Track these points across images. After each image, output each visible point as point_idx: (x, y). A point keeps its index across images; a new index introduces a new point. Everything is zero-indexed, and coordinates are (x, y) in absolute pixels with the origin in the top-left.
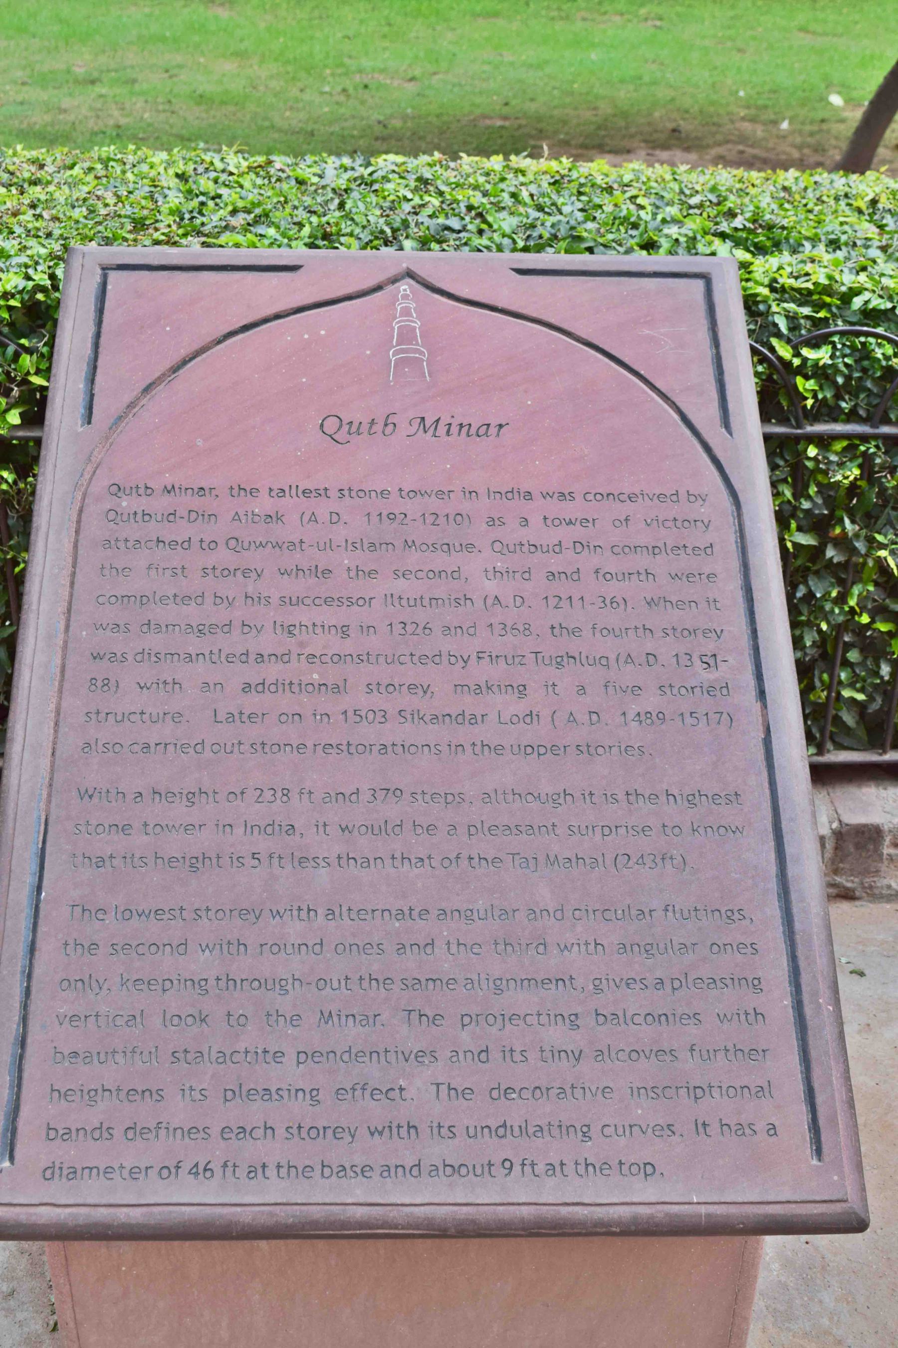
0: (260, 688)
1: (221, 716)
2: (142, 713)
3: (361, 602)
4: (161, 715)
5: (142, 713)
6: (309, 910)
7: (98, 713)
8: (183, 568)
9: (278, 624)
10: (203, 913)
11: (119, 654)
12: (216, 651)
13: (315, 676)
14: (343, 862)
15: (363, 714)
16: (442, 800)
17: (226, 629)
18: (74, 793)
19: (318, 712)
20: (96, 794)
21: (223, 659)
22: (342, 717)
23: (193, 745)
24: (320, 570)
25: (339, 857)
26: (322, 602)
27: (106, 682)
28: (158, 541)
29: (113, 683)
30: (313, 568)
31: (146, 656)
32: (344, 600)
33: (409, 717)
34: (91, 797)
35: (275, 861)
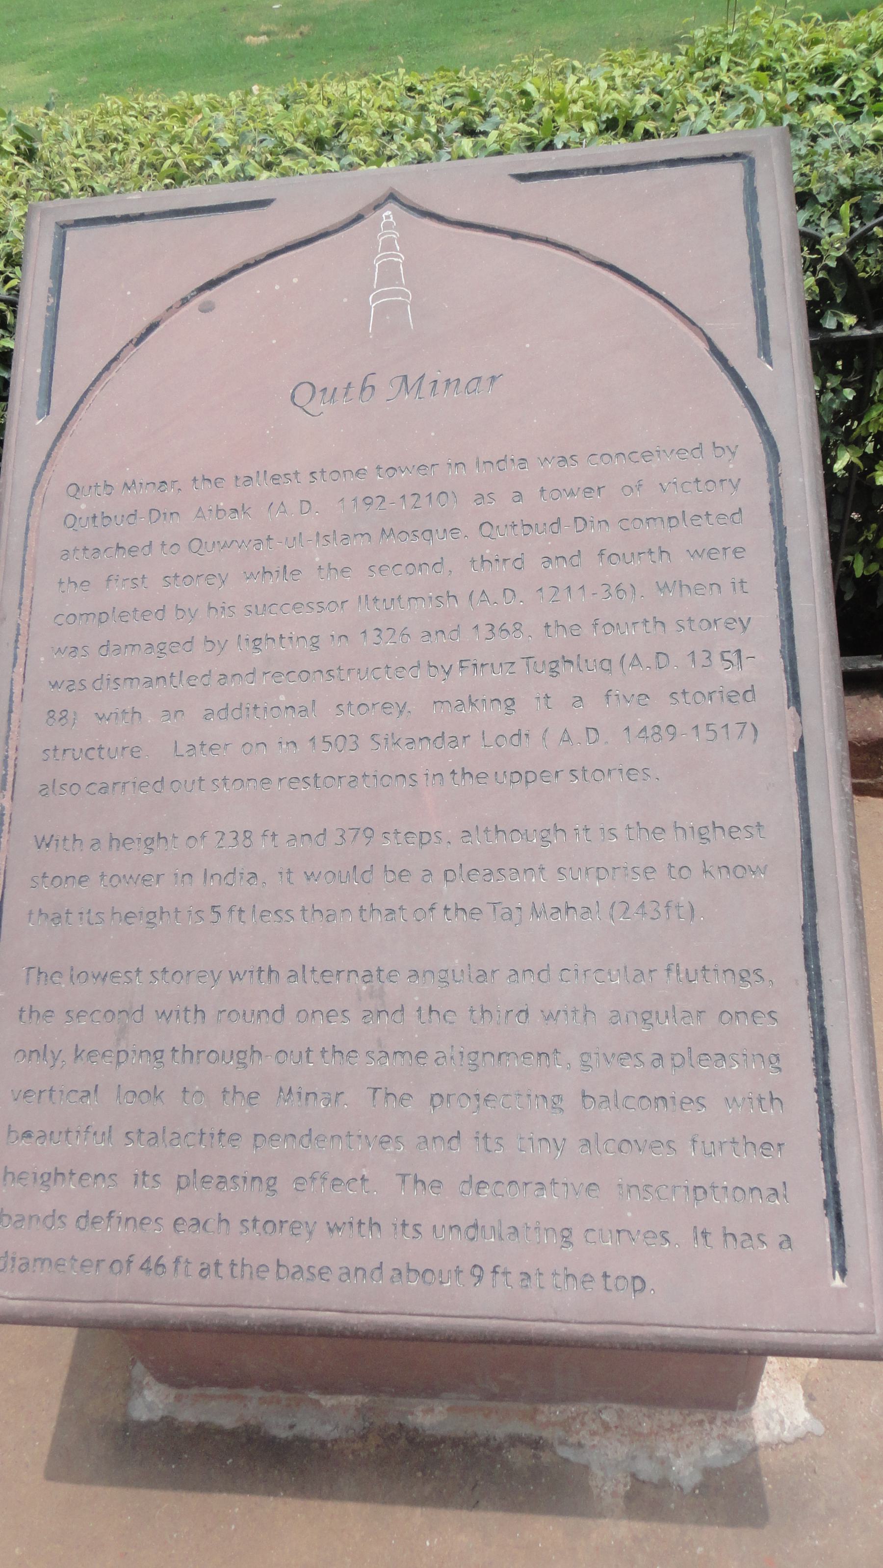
0: (223, 713)
1: (183, 749)
2: (101, 748)
3: (333, 606)
4: (120, 750)
5: (101, 748)
6: (270, 971)
7: (55, 750)
8: (144, 577)
9: (243, 638)
10: (159, 975)
11: (77, 682)
12: (177, 673)
13: (282, 698)
14: (308, 914)
15: (332, 740)
16: (416, 840)
17: (188, 646)
18: (32, 841)
19: (284, 741)
20: (53, 843)
21: (184, 681)
22: (309, 744)
23: (152, 783)
24: (289, 570)
25: (304, 910)
26: (290, 607)
27: (64, 714)
28: (118, 548)
29: (71, 716)
30: (281, 570)
31: (105, 682)
32: (315, 606)
33: (383, 742)
34: (48, 845)
35: (235, 914)
